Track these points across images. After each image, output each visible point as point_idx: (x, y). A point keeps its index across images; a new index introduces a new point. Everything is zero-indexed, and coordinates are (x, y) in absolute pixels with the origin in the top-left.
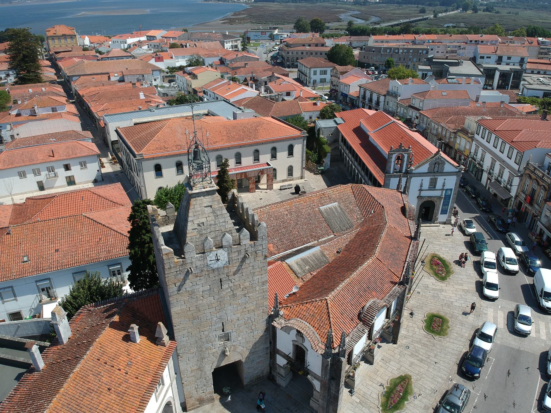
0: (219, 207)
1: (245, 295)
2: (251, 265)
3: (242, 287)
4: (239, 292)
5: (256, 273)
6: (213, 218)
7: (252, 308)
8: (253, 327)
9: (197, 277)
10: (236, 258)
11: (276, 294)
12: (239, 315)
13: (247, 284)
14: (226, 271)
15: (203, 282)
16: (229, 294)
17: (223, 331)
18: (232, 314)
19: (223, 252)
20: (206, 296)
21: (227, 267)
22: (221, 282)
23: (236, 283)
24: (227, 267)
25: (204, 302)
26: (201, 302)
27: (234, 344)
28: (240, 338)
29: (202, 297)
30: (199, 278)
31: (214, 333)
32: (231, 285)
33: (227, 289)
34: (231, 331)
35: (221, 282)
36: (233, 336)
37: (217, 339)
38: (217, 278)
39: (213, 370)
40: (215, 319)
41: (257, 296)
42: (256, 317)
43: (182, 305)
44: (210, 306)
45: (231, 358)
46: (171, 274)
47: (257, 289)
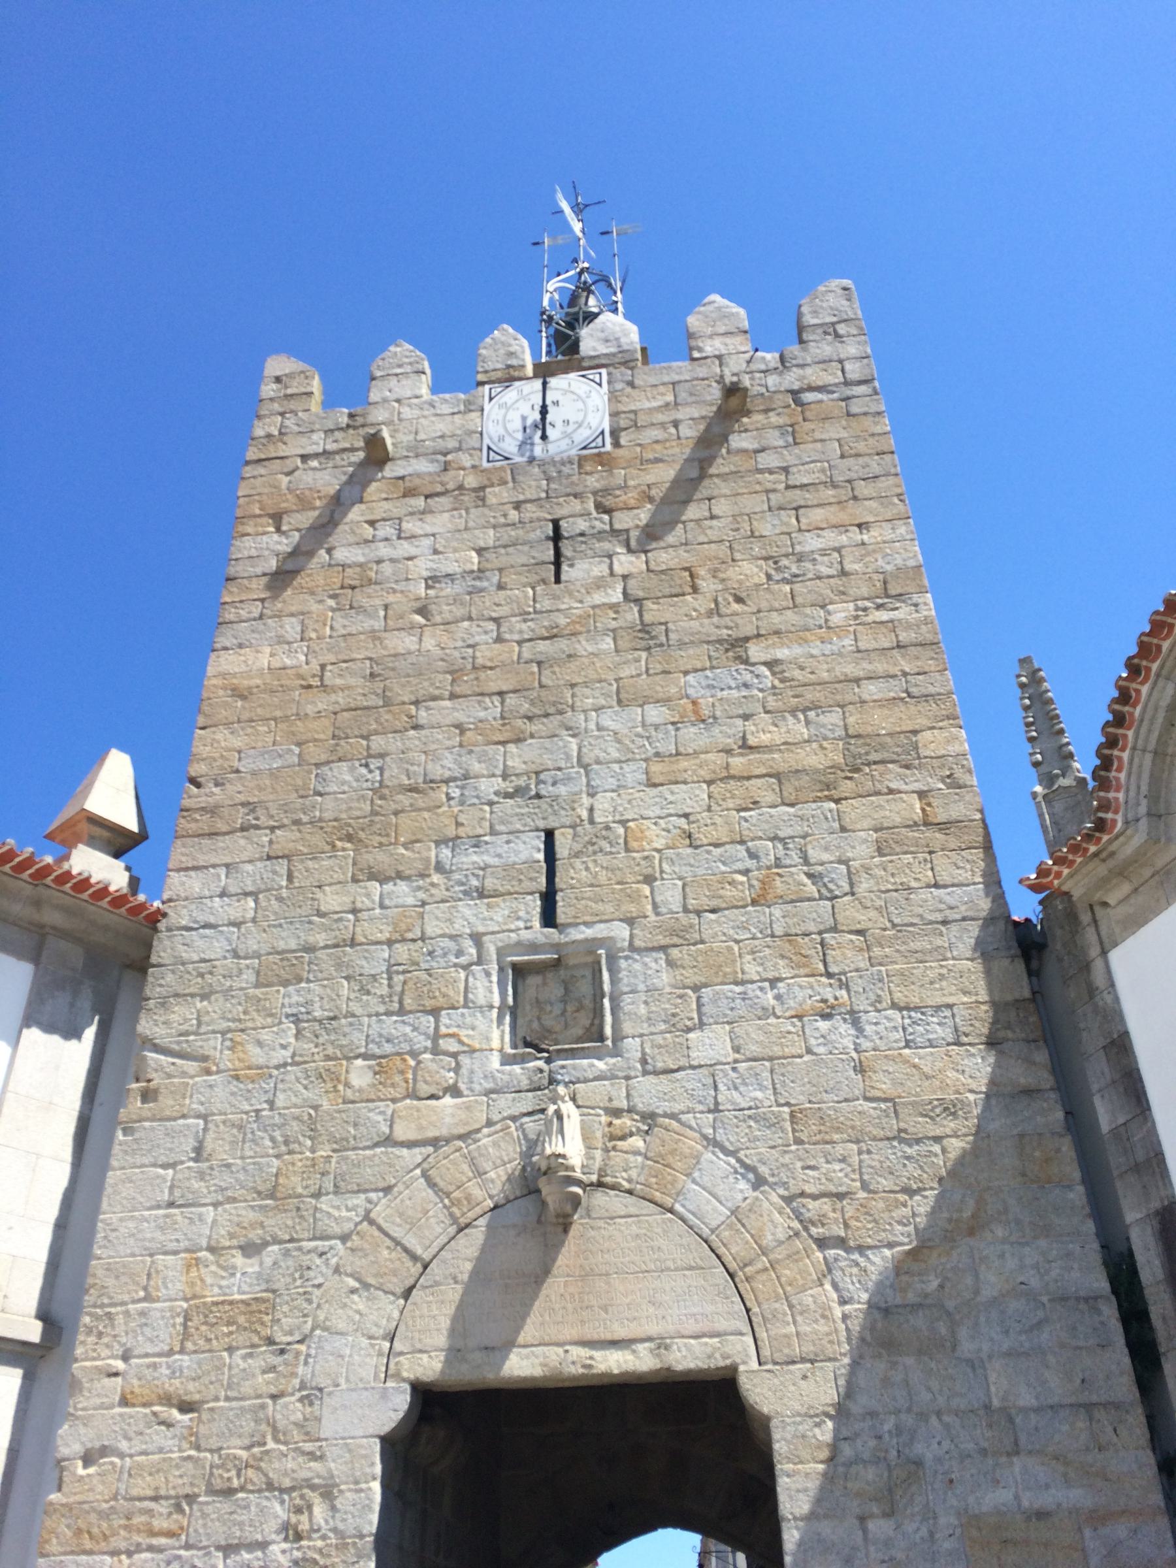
1: (736, 647)
2: (768, 460)
3: (707, 585)
4: (684, 617)
7: (812, 759)
8: (846, 955)
9: (409, 493)
11: (1025, 661)
13: (749, 571)
14: (593, 482)
15: (442, 522)
16: (608, 620)
17: (549, 917)
18: (633, 773)
20: (446, 611)
22: (557, 537)
24: (601, 459)
25: (429, 643)
26: (408, 642)
27: (649, 1092)
28: (710, 1045)
29: (422, 611)
30: (420, 502)
31: (470, 915)
33: (599, 584)
34: (621, 932)
36: (642, 989)
37: (488, 989)
40: (489, 787)
41: (851, 670)
42: (860, 849)
43: (281, 640)
44: (462, 678)
45: (622, 1314)
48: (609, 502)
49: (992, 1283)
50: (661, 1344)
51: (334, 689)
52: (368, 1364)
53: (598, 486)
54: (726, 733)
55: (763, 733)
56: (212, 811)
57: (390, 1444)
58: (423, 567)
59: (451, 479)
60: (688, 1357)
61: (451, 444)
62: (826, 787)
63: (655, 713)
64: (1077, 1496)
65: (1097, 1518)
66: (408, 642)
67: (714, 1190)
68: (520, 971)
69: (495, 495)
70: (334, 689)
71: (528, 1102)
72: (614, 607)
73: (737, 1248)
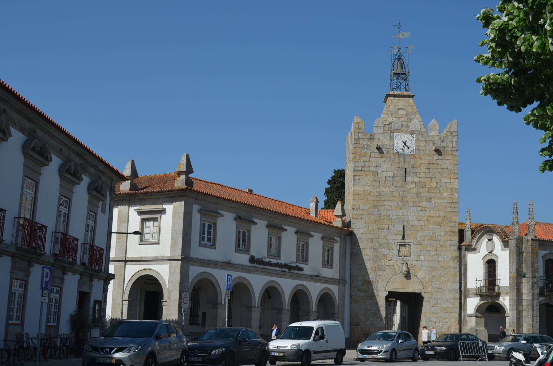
0: (414, 112)
3: (428, 186)
5: (445, 175)
6: (406, 120)
7: (439, 219)
8: (439, 249)
10: (423, 148)
12: (422, 223)
17: (403, 238)
19: (411, 138)
21: (414, 156)
22: (406, 172)
23: (423, 180)
26: (383, 189)
28: (422, 258)
32: (417, 179)
33: (412, 183)
35: (406, 172)
38: (401, 165)
39: (387, 294)
42: (443, 234)
46: (359, 146)
47: (445, 195)
48: (414, 166)
49: (448, 287)
50: (415, 290)
51: (372, 196)
52: (383, 289)
53: (413, 162)
54: (427, 213)
55: (432, 213)
56: (358, 214)
57: (386, 297)
58: (385, 174)
59: (389, 156)
60: (417, 291)
61: (389, 147)
62: (440, 224)
63: (419, 209)
64: (452, 306)
65: (453, 308)
66: (383, 189)
67: (421, 275)
68: (400, 245)
69: (397, 160)
70: (372, 196)
71: (400, 262)
72: (414, 188)
73: (423, 281)
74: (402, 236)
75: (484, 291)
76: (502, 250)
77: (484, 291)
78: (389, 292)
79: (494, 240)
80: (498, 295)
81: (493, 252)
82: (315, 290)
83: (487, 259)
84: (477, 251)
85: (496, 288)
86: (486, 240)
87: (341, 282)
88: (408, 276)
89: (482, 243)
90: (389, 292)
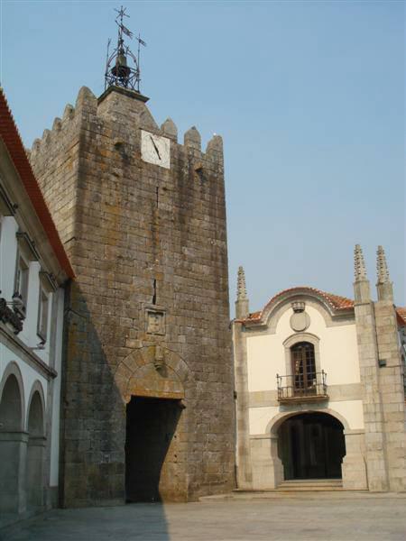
17: (154, 302)
74: (152, 297)
75: (289, 393)
76: (327, 327)
77: (289, 393)
78: (132, 396)
79: (306, 310)
80: (325, 400)
81: (307, 331)
82: (30, 378)
83: (294, 341)
84: (270, 330)
85: (320, 391)
86: (291, 311)
87: (50, 375)
88: (161, 368)
89: (279, 317)
90: (132, 396)
